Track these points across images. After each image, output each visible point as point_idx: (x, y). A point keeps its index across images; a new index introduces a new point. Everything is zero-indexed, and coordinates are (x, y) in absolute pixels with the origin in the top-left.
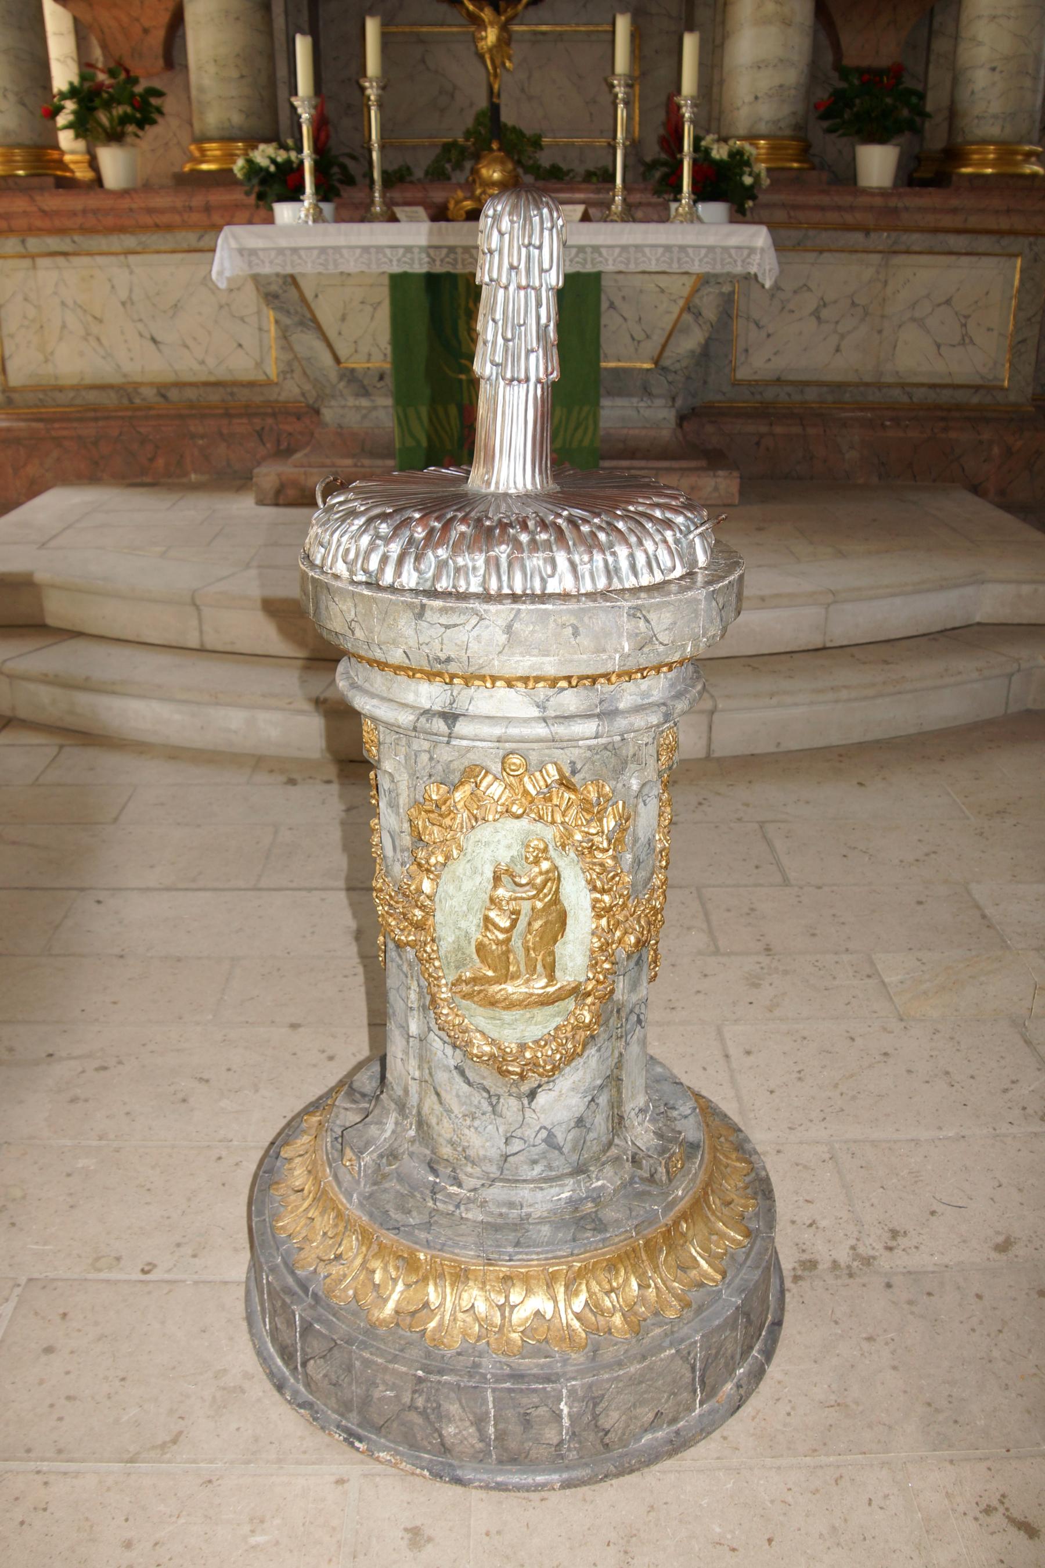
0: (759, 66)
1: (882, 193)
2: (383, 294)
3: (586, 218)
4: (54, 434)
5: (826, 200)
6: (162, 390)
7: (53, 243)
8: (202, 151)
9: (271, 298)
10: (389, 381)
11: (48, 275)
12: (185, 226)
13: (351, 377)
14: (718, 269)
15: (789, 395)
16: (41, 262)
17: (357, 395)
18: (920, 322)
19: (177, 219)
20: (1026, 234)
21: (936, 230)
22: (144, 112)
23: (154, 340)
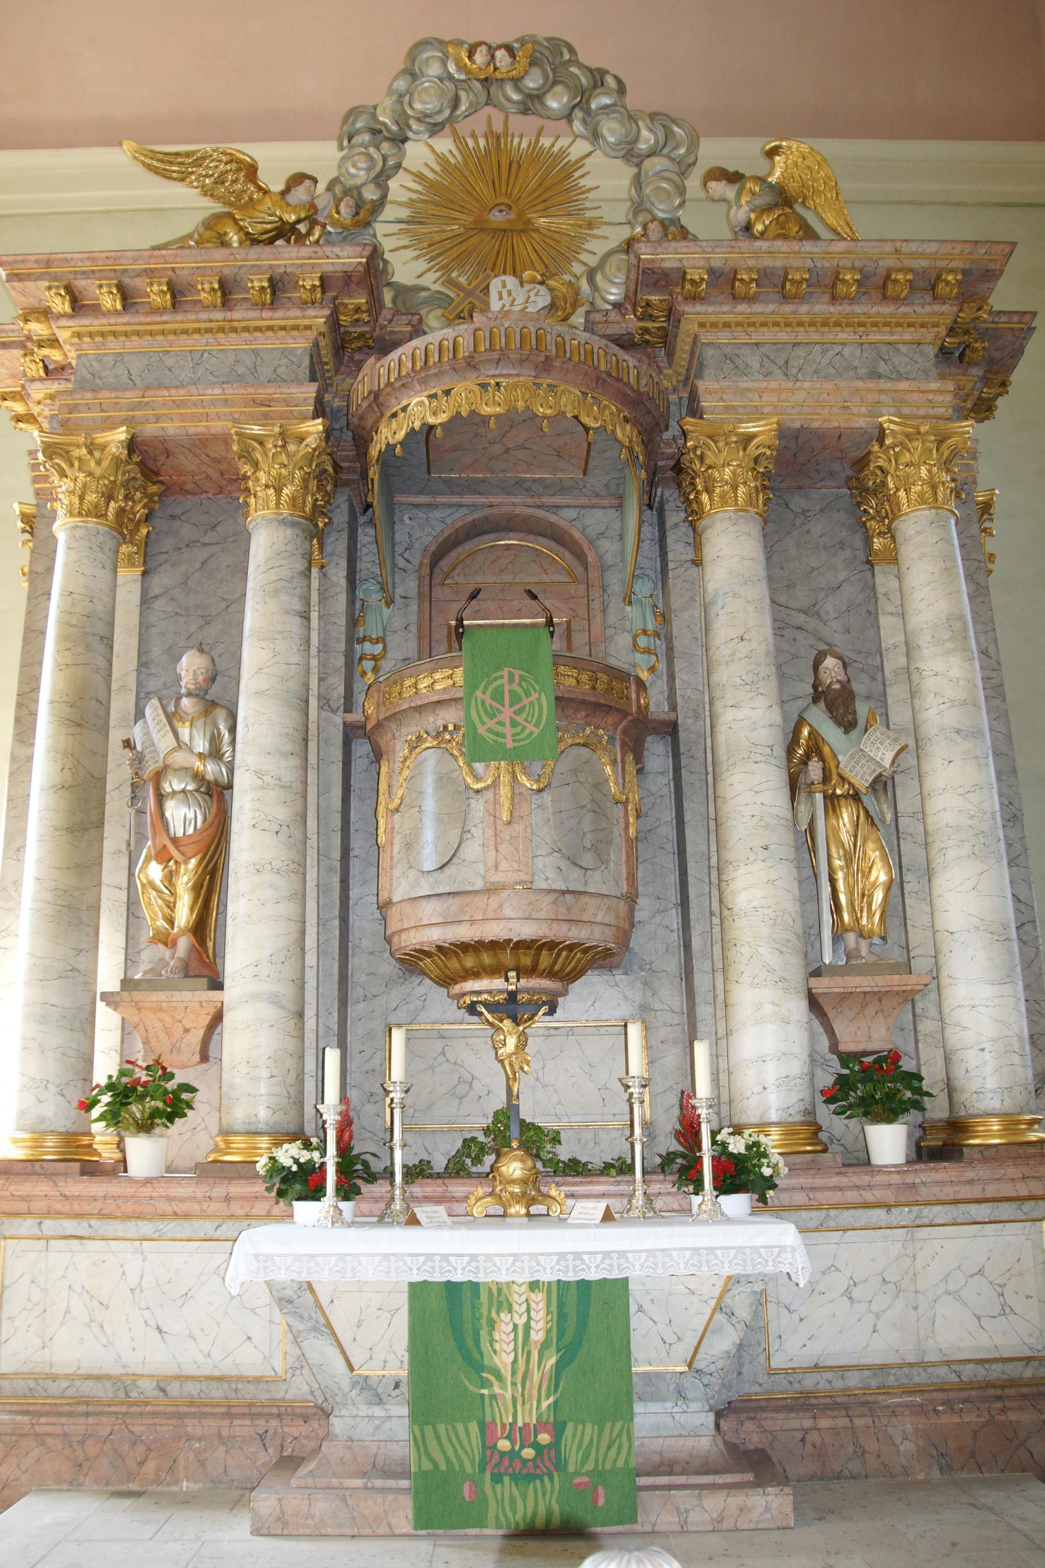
1: (898, 1170)
3: (608, 1217)
4: (37, 1429)
5: (843, 1181)
7: (70, 1226)
8: (228, 1143)
9: (284, 1302)
10: (404, 1388)
11: (60, 1255)
12: (204, 1215)
13: (364, 1384)
14: (749, 1270)
15: (830, 1382)
18: (956, 1295)
19: (197, 1207)
21: (956, 1202)
22: (175, 1106)
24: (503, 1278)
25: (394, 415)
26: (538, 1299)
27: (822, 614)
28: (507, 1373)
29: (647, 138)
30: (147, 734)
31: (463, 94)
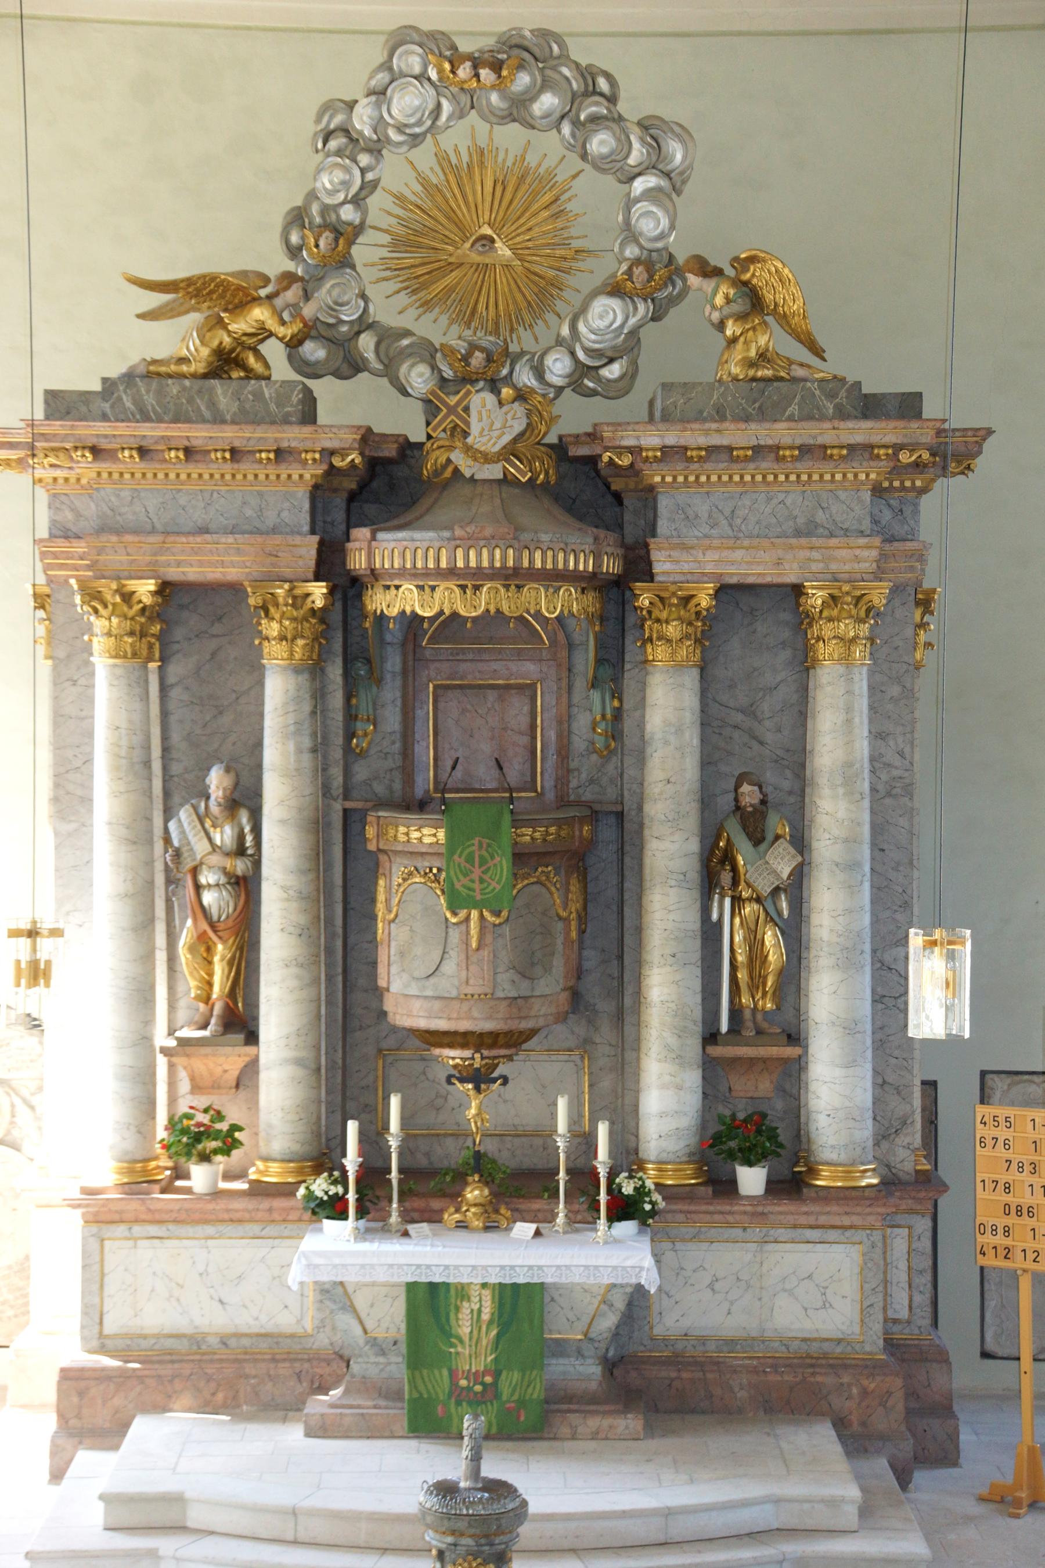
0: (662, 1115)
3: (538, 1233)
5: (711, 1208)
7: (153, 1230)
13: (373, 1342)
14: (620, 1281)
16: (140, 1243)
17: (377, 1355)
18: (790, 1292)
20: (864, 1228)
21: (795, 1227)
23: (221, 1301)
24: (465, 1280)
25: (388, 587)
26: (487, 1294)
27: (759, 714)
28: (466, 1340)
29: (637, 154)
30: (183, 832)
31: (446, 105)
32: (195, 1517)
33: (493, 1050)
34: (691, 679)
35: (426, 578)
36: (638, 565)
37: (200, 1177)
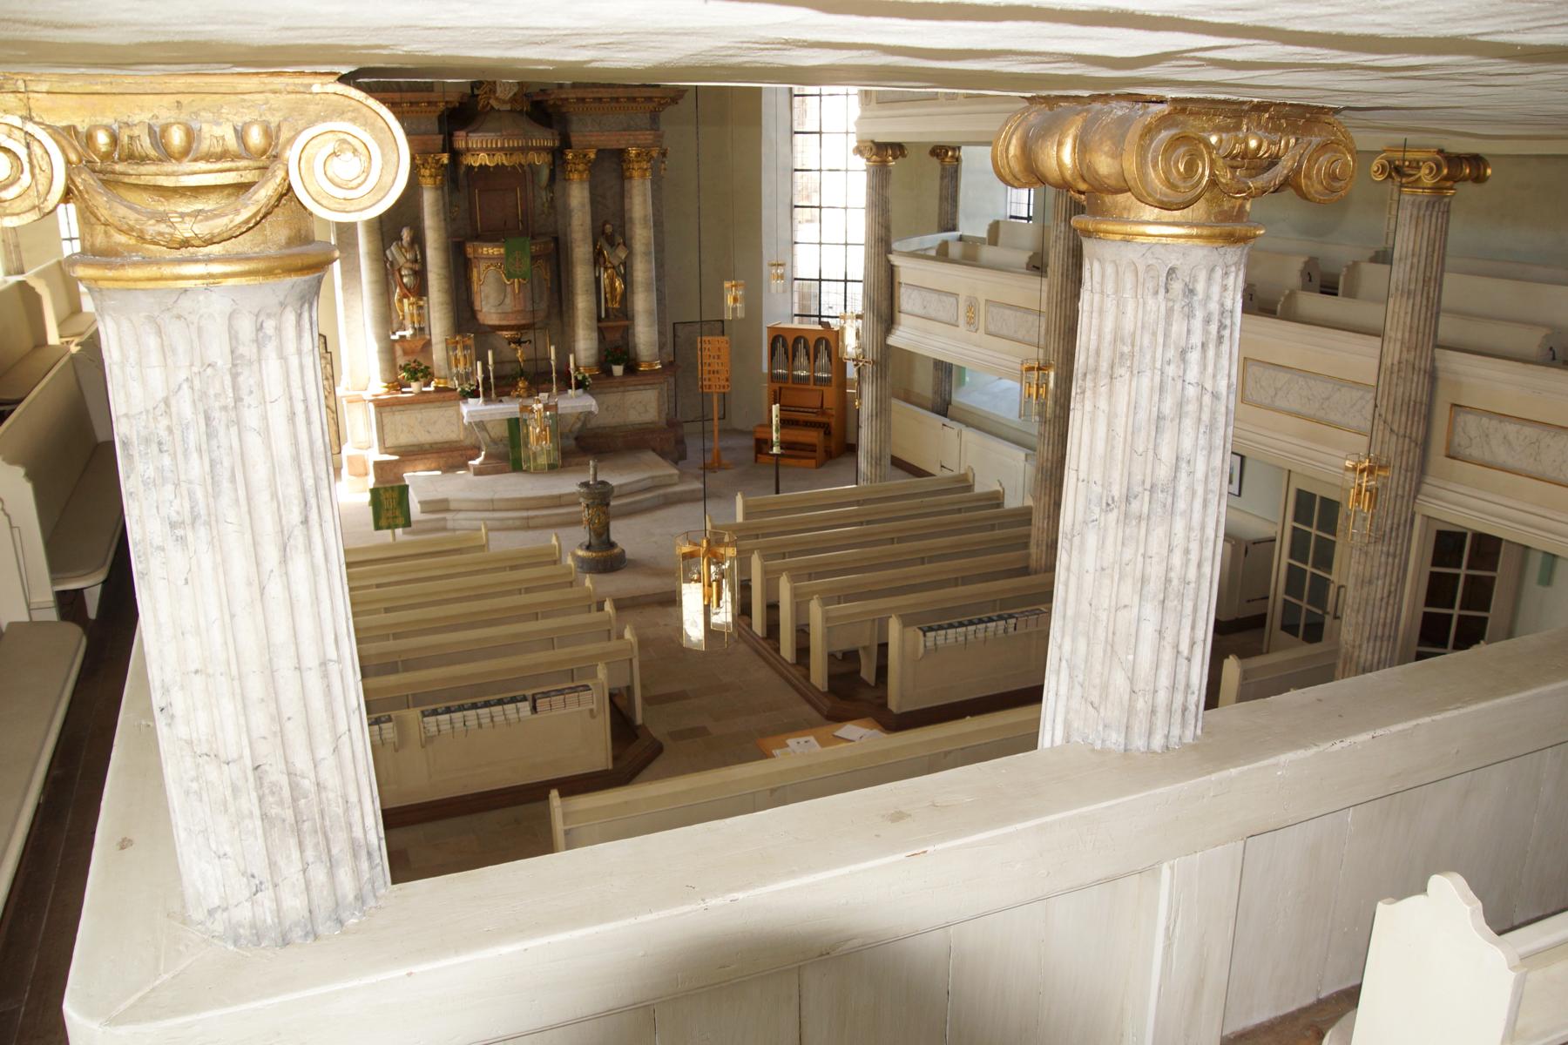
2: (506, 425)
6: (431, 445)
32: (453, 506)
33: (520, 333)
34: (586, 186)
35: (491, 152)
36: (566, 143)
37: (415, 387)
